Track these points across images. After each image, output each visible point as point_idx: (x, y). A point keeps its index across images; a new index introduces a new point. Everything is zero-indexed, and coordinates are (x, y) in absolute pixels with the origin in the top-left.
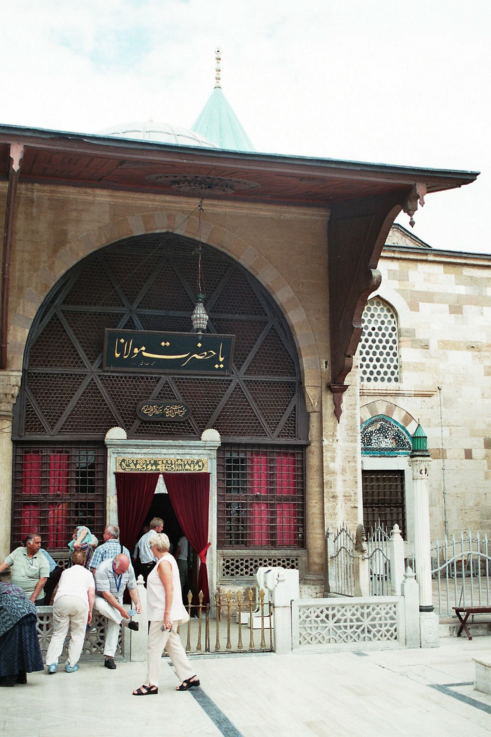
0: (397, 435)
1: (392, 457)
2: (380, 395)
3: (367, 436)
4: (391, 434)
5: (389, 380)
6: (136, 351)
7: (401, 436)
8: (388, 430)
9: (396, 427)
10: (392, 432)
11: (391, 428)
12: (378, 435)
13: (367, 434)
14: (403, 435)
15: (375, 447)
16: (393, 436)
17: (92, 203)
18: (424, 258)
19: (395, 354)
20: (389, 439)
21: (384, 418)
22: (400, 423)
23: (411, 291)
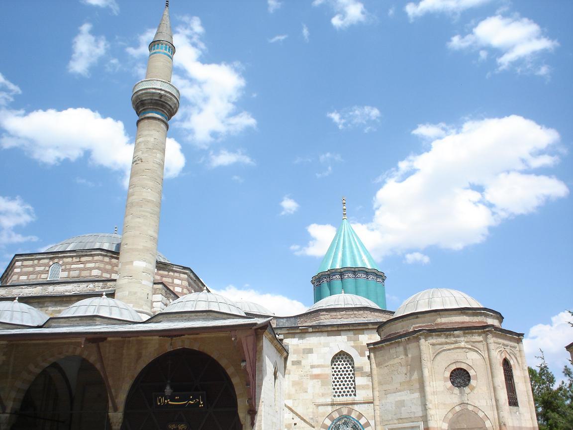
2: (344, 404)
4: (350, 425)
5: (350, 395)
6: (166, 401)
17: (152, 340)
18: (367, 327)
19: (354, 381)
21: (346, 417)
23: (361, 346)
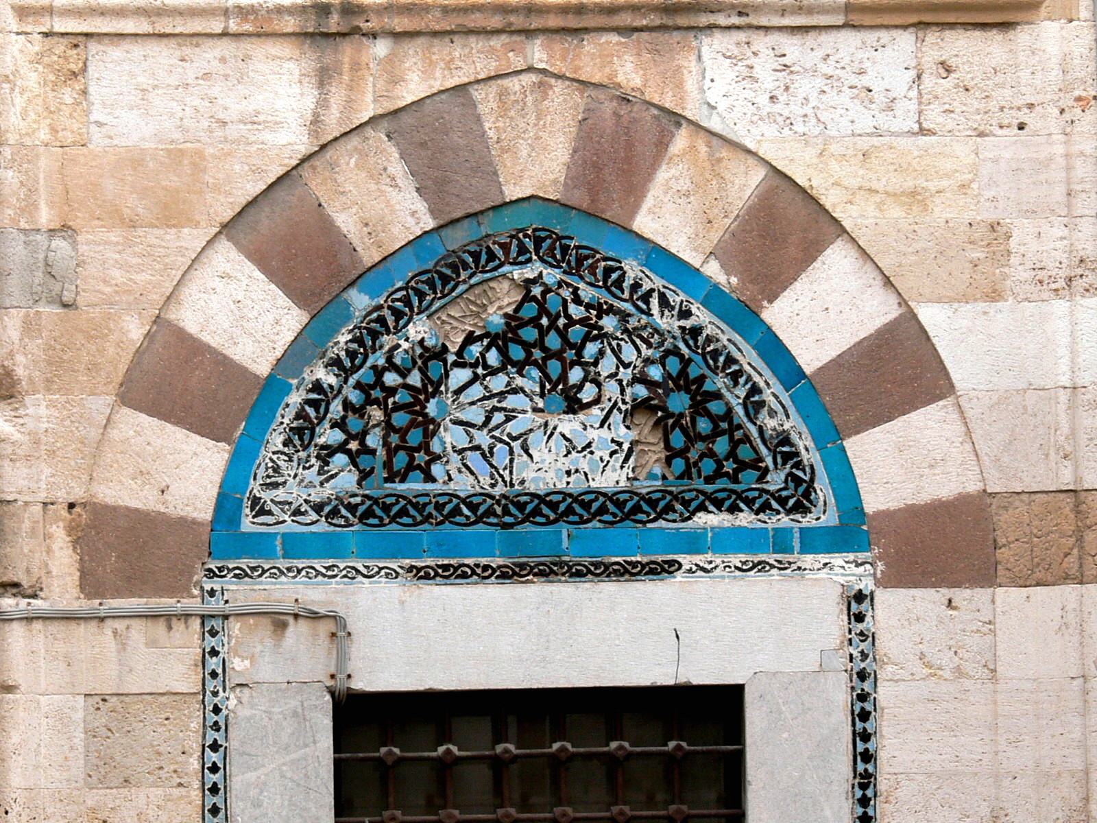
0: (682, 381)
1: (626, 572)
3: (392, 391)
7: (719, 382)
8: (594, 332)
9: (664, 302)
10: (629, 354)
11: (624, 317)
12: (498, 383)
13: (391, 379)
14: (735, 376)
15: (463, 485)
16: (642, 391)
20: (597, 413)
22: (713, 270)
